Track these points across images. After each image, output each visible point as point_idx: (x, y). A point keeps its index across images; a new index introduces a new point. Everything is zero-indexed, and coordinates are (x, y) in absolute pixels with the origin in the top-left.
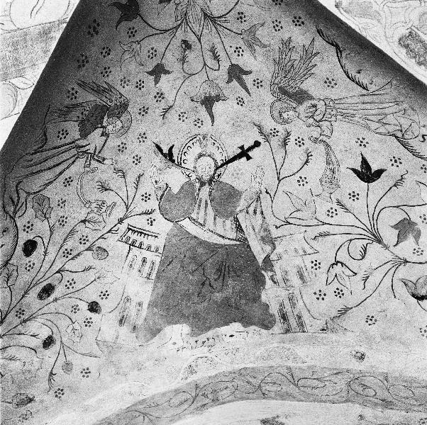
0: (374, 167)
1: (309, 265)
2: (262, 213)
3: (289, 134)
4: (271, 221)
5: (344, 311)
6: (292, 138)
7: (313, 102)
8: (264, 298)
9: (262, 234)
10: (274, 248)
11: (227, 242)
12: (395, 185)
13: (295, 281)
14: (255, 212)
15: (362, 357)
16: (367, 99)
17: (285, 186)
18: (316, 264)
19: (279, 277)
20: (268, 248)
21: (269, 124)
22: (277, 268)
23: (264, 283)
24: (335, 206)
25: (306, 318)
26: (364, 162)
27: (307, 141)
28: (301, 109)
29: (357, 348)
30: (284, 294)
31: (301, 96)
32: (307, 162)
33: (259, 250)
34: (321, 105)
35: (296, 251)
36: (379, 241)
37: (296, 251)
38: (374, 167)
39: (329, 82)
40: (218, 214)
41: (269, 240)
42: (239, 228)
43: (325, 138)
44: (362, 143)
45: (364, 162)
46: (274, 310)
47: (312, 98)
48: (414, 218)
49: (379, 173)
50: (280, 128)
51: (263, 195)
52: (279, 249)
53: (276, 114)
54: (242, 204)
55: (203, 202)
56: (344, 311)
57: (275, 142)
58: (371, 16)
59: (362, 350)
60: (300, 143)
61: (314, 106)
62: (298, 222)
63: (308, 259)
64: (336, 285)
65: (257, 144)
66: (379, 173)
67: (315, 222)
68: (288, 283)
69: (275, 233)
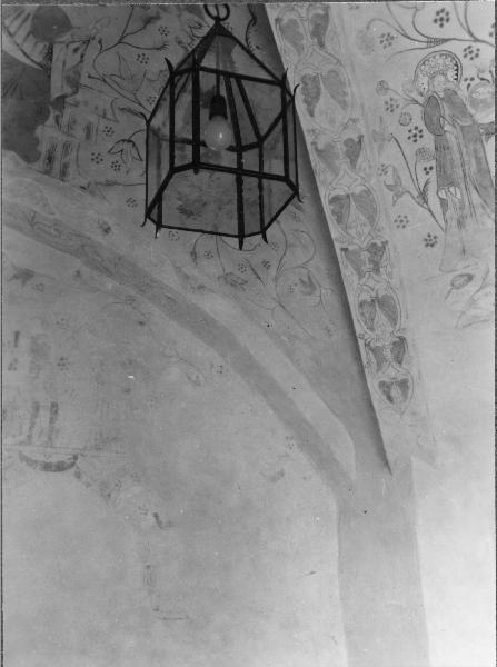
1: (102, 127)
2: (82, 56)
4: (86, 69)
5: (109, 184)
6: (159, 23)
7: (201, 21)
8: (39, 131)
9: (71, 74)
10: (76, 92)
11: (27, 62)
13: (80, 133)
14: (76, 50)
15: (107, 231)
17: (122, 49)
18: (109, 131)
19: (65, 120)
20: (68, 90)
22: (68, 111)
23: (47, 118)
25: (72, 170)
29: (106, 219)
30: (61, 138)
32: (158, 49)
33: (58, 86)
35: (96, 108)
37: (96, 108)
40: (33, 32)
41: (76, 86)
42: (49, 55)
46: (43, 148)
51: (94, 43)
52: (79, 97)
54: (66, 37)
55: (23, 16)
56: (109, 184)
58: (295, 45)
59: (111, 223)
60: (164, 31)
61: (201, 26)
62: (115, 86)
63: (103, 124)
64: (117, 157)
67: (131, 97)
68: (72, 132)
69: (84, 80)
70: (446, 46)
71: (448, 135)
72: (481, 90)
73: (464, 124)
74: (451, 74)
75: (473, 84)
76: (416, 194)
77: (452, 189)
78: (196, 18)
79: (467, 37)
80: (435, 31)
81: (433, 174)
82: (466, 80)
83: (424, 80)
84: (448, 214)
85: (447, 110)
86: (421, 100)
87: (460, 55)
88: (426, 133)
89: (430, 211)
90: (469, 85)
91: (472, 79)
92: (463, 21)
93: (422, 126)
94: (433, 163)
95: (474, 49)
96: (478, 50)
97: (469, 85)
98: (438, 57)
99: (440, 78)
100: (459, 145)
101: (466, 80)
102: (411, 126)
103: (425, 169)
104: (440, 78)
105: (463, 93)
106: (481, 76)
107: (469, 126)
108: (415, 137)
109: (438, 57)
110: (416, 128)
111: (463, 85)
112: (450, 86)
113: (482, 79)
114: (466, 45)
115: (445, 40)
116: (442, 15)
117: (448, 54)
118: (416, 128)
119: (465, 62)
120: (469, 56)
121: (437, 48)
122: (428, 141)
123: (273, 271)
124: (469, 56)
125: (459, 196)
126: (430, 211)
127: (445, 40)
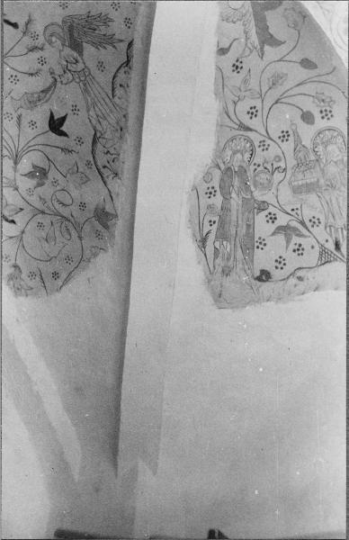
0: (64, 128)
3: (42, 49)
7: (79, 58)
12: (62, 149)
16: (107, 100)
21: (38, 27)
24: (15, 116)
26: (63, 119)
27: (46, 68)
28: (68, 51)
31: (76, 46)
32: (32, 75)
34: (80, 66)
36: (16, 163)
38: (64, 128)
39: (101, 65)
43: (59, 80)
44: (75, 109)
45: (63, 119)
47: (81, 53)
48: (50, 175)
49: (63, 134)
50: (41, 40)
53: (48, 32)
57: (27, 40)
60: (42, 61)
61: (77, 61)
65: (15, 25)
66: (63, 134)
70: (249, 134)
71: (232, 201)
72: (263, 176)
73: (244, 196)
74: (247, 155)
75: (259, 169)
76: (199, 239)
77: (225, 243)
78: (75, 54)
79: (265, 133)
80: (246, 120)
81: (215, 227)
82: (255, 164)
83: (229, 153)
84: (217, 261)
85: (236, 182)
86: (223, 167)
87: (257, 144)
88: (218, 193)
89: (205, 255)
90: (256, 169)
91: (259, 166)
92: (265, 121)
93: (217, 188)
94: (217, 219)
95: (266, 143)
96: (269, 145)
97: (256, 169)
98: (242, 140)
99: (239, 156)
100: (237, 210)
101: (255, 164)
102: (210, 185)
103: (210, 221)
104: (239, 156)
105: (250, 173)
106: (266, 165)
107: (248, 199)
108: (211, 194)
109: (242, 140)
110: (213, 188)
111: (252, 168)
112: (244, 165)
113: (265, 168)
114: (262, 139)
115: (251, 130)
116: (254, 110)
117: (248, 140)
118: (213, 188)
119: (258, 150)
120: (262, 148)
121: (241, 133)
122: (218, 200)
123: (60, 282)
124: (262, 148)
125: (228, 249)
126: (205, 255)
127: (251, 130)
